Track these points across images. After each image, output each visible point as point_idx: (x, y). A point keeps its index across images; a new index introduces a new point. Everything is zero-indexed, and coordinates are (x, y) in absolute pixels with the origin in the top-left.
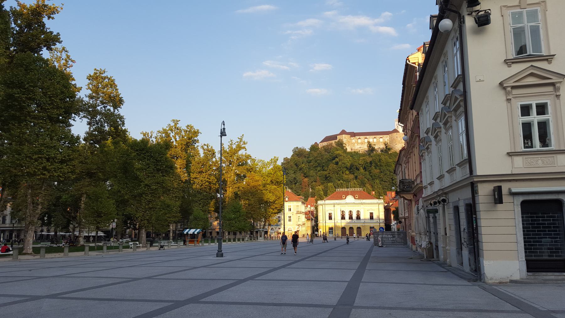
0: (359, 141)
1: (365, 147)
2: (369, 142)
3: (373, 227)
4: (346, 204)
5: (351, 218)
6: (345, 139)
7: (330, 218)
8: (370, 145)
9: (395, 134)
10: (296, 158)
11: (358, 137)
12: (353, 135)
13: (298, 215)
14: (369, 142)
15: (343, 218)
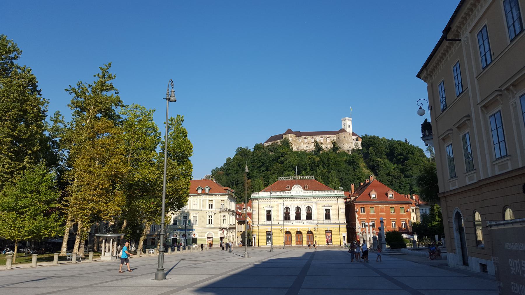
0: (306, 141)
1: (312, 147)
2: (316, 141)
3: (330, 232)
4: (293, 197)
5: (298, 217)
6: (291, 138)
7: (269, 218)
8: (317, 144)
9: (342, 134)
10: (239, 156)
11: (304, 137)
12: (299, 134)
13: (223, 214)
14: (316, 141)
15: (287, 217)
